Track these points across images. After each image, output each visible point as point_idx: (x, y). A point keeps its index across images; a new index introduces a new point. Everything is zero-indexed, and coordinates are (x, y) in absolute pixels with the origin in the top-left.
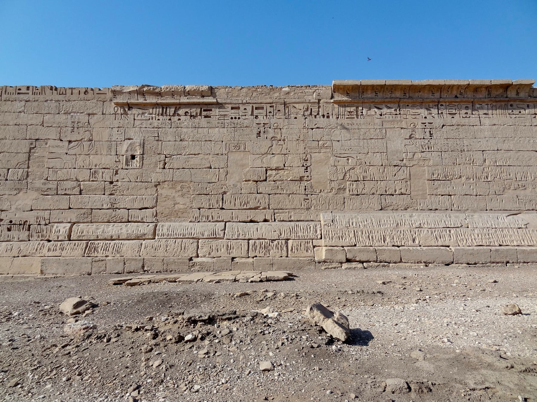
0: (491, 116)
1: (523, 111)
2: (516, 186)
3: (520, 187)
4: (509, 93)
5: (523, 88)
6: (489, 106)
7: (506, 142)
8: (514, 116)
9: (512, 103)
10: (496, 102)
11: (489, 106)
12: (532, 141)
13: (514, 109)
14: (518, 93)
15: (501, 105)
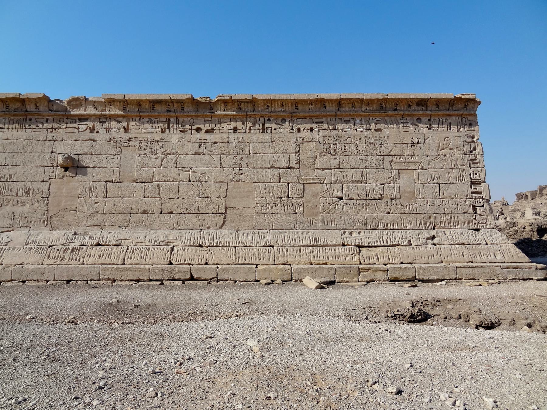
0: (6, 130)
1: (41, 126)
2: (15, 203)
3: (19, 203)
4: (28, 107)
5: (40, 102)
6: (7, 120)
7: (15, 157)
8: (30, 130)
9: (31, 117)
10: (15, 115)
11: (7, 120)
12: (42, 156)
13: (32, 123)
14: (37, 107)
15: (19, 120)
